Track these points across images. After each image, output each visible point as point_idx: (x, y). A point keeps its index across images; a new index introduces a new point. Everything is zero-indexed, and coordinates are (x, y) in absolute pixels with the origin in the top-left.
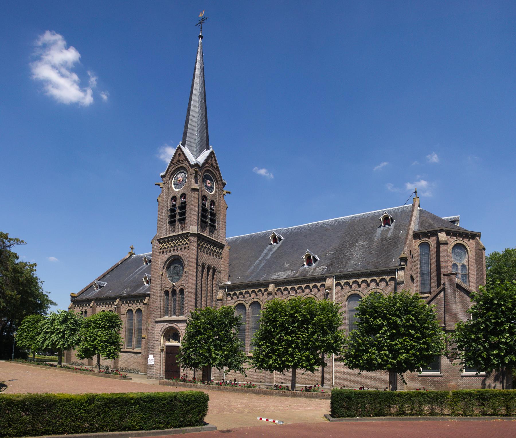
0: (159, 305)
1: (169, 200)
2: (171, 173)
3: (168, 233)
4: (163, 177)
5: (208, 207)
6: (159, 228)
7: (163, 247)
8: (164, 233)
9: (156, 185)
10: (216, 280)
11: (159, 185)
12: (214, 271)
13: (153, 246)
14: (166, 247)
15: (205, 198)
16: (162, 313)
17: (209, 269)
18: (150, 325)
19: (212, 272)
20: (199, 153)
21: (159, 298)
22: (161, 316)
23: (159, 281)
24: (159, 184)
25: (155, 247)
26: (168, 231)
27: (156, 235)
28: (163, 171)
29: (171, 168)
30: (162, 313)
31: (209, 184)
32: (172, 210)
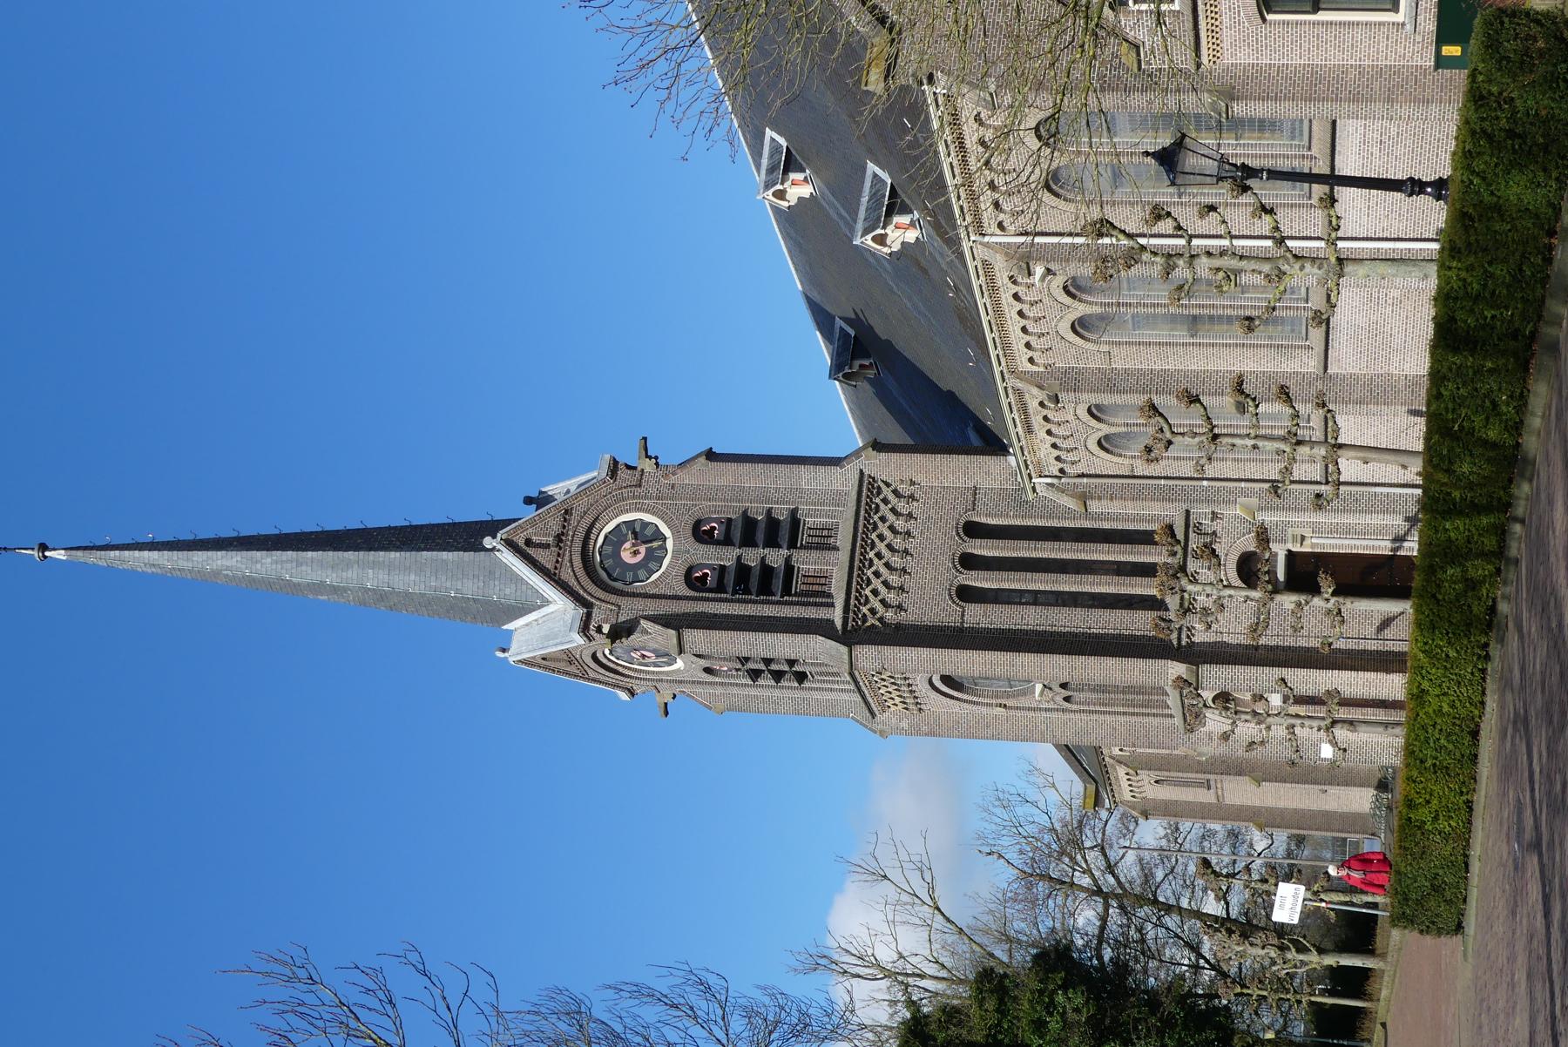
0: (1122, 719)
1: (717, 680)
2: (617, 677)
3: (847, 687)
4: (632, 693)
5: (727, 557)
6: (831, 711)
7: (901, 706)
8: (845, 696)
9: (667, 714)
10: (1007, 516)
11: (666, 704)
12: (973, 530)
13: (900, 731)
14: (898, 700)
15: (694, 581)
16: (1154, 711)
17: (969, 562)
18: (1205, 749)
19: (978, 542)
20: (524, 587)
21: (1095, 717)
22: (1167, 711)
23: (1031, 714)
24: (663, 705)
25: (904, 724)
26: (836, 686)
27: (857, 721)
28: (616, 695)
29: (602, 678)
30: (1154, 711)
31: (636, 553)
32: (755, 675)
